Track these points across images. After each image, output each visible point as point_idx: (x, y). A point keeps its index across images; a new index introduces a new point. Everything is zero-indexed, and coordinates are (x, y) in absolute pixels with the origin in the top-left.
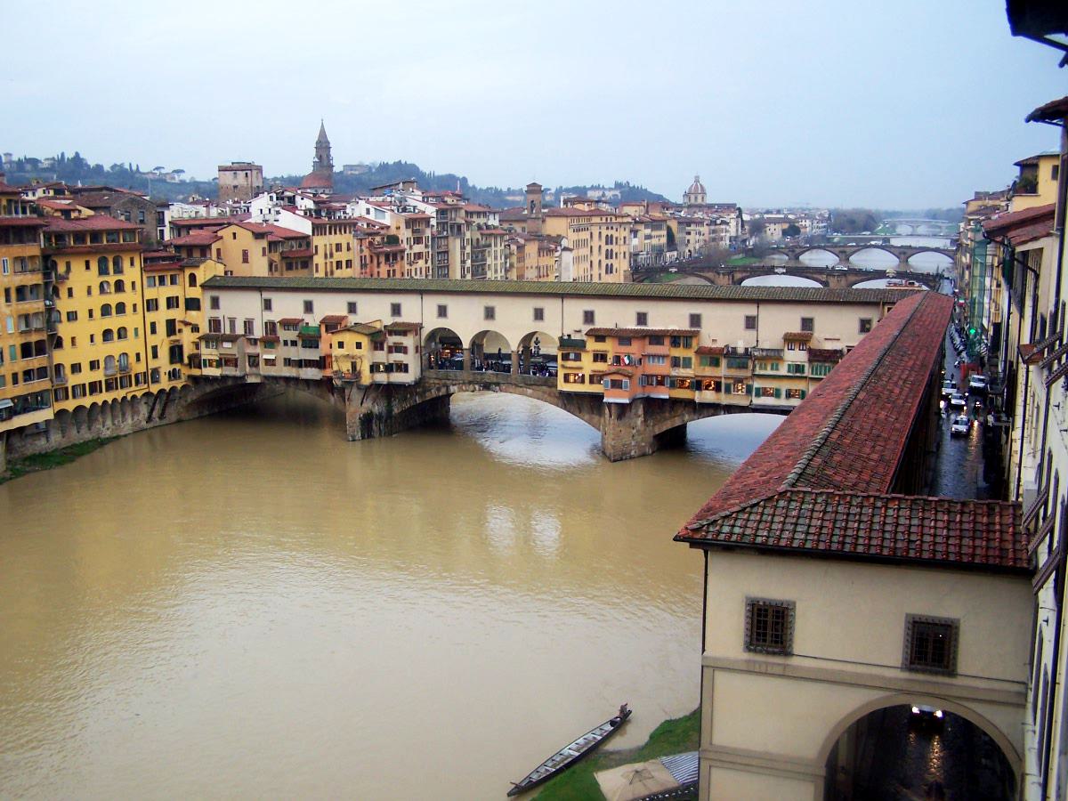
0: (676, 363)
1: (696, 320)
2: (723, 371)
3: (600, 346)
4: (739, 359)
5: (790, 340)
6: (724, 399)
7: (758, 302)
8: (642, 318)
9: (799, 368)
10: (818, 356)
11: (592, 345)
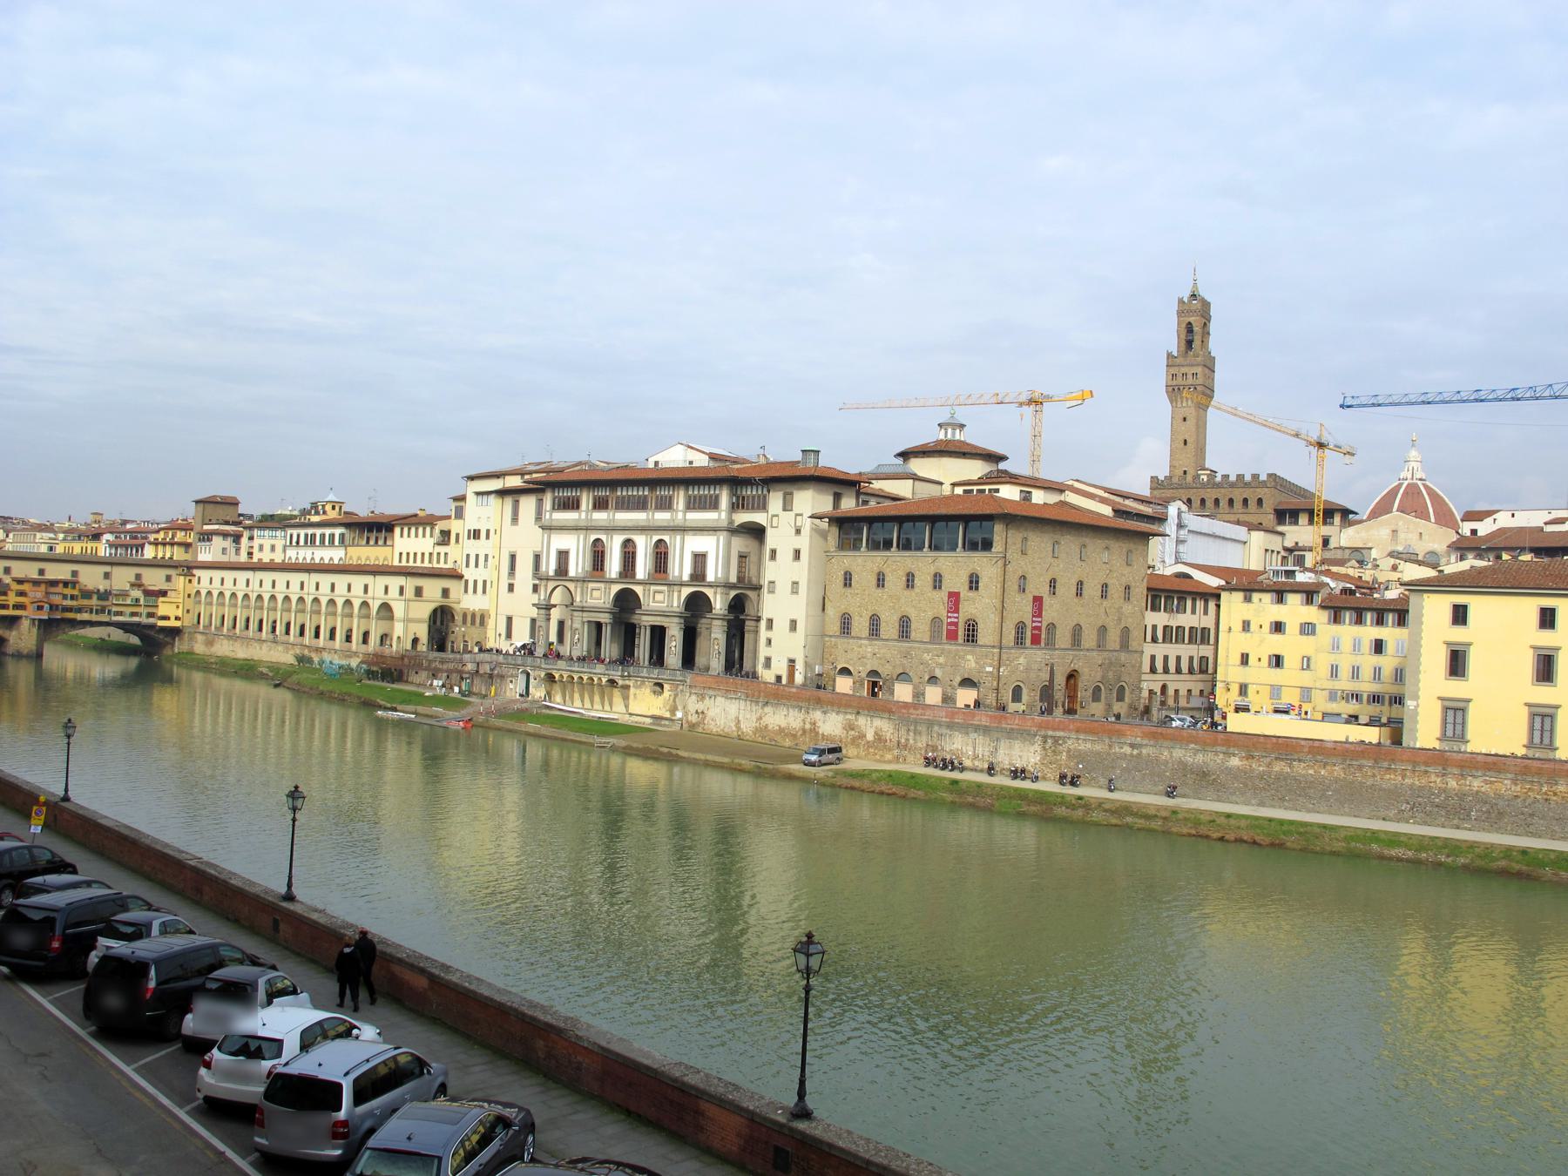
0: (65, 597)
1: (75, 573)
2: (94, 601)
3: (21, 587)
4: (105, 595)
5: (132, 585)
6: (94, 618)
7: (112, 564)
8: (41, 572)
9: (137, 600)
10: (147, 593)
11: (15, 586)
